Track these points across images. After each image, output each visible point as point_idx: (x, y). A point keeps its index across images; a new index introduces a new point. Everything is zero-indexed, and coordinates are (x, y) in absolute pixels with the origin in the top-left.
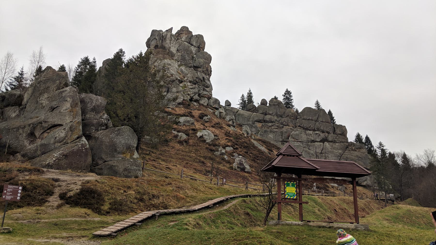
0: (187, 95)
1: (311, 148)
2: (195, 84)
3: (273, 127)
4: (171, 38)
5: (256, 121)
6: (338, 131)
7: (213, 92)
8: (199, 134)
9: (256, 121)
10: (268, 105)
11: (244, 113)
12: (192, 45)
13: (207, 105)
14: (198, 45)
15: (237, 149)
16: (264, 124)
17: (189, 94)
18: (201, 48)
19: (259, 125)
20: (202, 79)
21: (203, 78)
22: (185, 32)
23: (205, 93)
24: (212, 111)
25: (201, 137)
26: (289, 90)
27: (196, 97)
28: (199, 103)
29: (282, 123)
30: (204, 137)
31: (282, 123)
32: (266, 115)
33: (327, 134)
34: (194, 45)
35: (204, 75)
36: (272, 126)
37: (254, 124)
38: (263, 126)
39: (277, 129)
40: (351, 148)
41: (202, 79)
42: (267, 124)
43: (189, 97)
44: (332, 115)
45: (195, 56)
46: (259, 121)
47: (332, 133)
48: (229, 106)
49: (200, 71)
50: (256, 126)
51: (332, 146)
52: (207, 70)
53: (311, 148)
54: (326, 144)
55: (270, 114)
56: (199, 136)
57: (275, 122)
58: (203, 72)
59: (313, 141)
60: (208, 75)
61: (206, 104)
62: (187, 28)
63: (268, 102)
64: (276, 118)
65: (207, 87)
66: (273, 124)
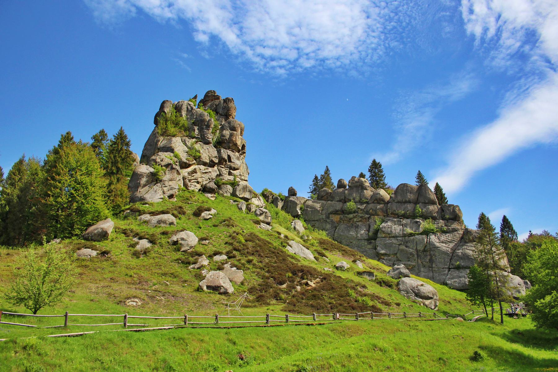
1: (409, 244)
3: (355, 220)
9: (331, 213)
10: (347, 187)
15: (234, 257)
16: (342, 216)
17: (198, 183)
19: (336, 218)
21: (229, 157)
26: (377, 161)
29: (367, 213)
32: (345, 202)
36: (354, 217)
37: (328, 218)
39: (361, 221)
42: (347, 215)
44: (441, 190)
46: (336, 212)
50: (332, 221)
53: (409, 244)
66: (355, 215)
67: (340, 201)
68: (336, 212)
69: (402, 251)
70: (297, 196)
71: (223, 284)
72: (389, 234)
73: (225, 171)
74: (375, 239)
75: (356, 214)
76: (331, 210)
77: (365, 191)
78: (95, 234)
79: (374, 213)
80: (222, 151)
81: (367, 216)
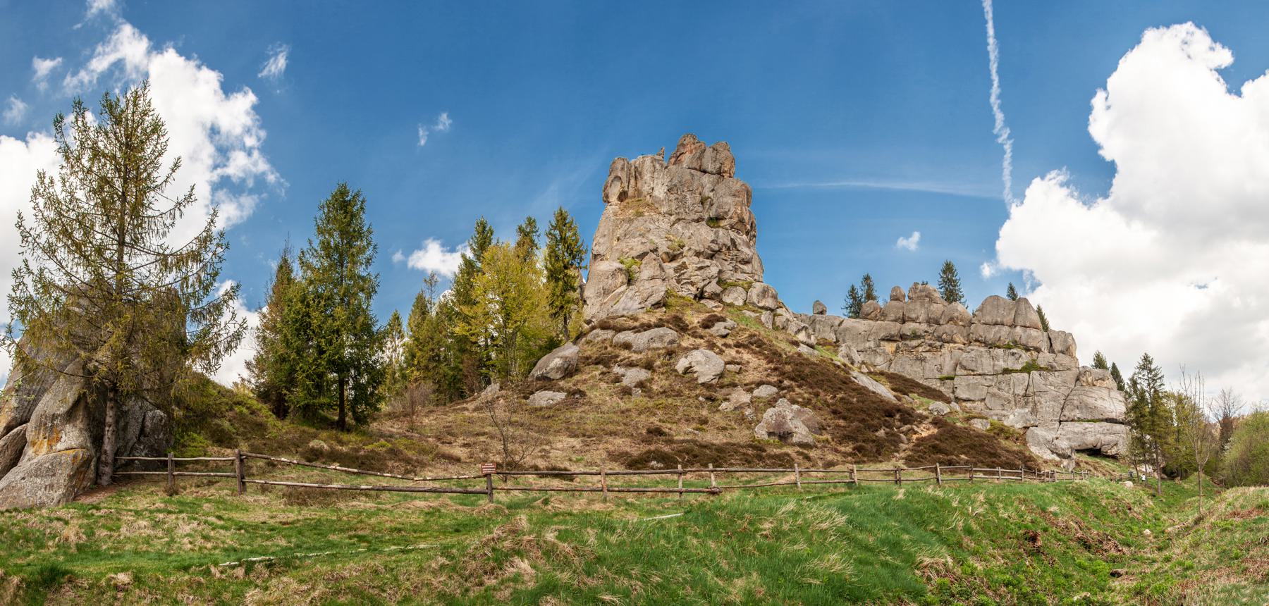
2: (711, 257)
3: (921, 349)
5: (883, 340)
13: (745, 303)
17: (692, 284)
19: (889, 347)
20: (729, 243)
24: (753, 315)
25: (688, 370)
27: (713, 287)
28: (721, 301)
29: (939, 338)
30: (695, 369)
31: (939, 338)
37: (879, 346)
38: (898, 348)
43: (693, 289)
46: (890, 339)
48: (822, 313)
55: (913, 321)
61: (740, 303)
64: (924, 326)
65: (746, 262)
67: (895, 321)
69: (994, 395)
73: (728, 267)
74: (952, 379)
76: (882, 335)
79: (949, 338)
81: (938, 344)
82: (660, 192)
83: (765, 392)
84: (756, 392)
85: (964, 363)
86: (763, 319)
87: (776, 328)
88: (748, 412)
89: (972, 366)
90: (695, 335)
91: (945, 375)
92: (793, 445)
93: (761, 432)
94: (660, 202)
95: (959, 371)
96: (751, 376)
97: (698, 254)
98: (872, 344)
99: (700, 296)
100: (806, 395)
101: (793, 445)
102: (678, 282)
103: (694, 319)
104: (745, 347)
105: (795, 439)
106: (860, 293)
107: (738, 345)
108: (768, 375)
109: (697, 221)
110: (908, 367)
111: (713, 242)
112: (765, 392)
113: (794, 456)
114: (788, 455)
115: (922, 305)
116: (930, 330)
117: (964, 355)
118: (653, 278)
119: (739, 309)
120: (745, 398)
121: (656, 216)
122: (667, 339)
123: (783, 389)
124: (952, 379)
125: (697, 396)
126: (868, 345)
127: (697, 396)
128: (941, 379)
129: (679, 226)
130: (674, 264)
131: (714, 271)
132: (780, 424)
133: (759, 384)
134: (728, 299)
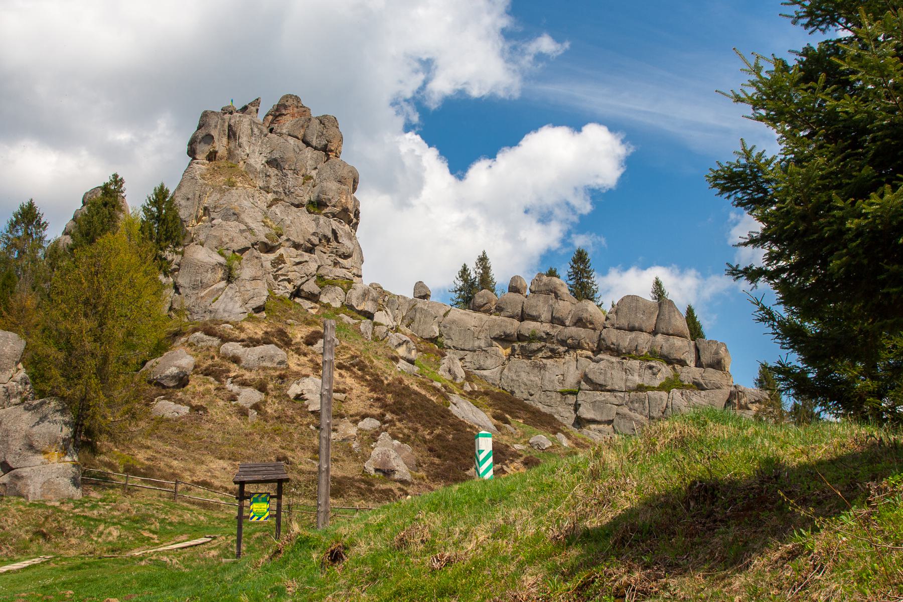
0: (286, 283)
2: (310, 250)
3: (540, 355)
4: (252, 129)
5: (495, 339)
6: (706, 358)
7: (365, 269)
8: (294, 390)
9: (495, 339)
11: (464, 317)
12: (308, 144)
14: (325, 142)
17: (289, 281)
18: (331, 151)
20: (330, 235)
21: (334, 232)
22: (290, 110)
23: (339, 272)
24: (352, 321)
25: (299, 397)
27: (311, 286)
29: (563, 342)
30: (307, 396)
31: (563, 342)
33: (678, 367)
34: (314, 144)
35: (334, 224)
38: (513, 350)
40: (736, 401)
41: (330, 235)
43: (290, 288)
45: (314, 173)
46: (504, 339)
47: (692, 364)
49: (326, 215)
51: (689, 399)
52: (345, 210)
54: (676, 393)
56: (292, 396)
57: (545, 340)
58: (334, 216)
59: (641, 388)
60: (349, 222)
61: (337, 304)
62: (297, 99)
63: (529, 285)
64: (547, 327)
65: (346, 257)
68: (504, 339)
70: (431, 299)
71: (397, 468)
72: (601, 385)
73: (327, 260)
75: (543, 343)
76: (497, 332)
77: (561, 302)
78: (167, 376)
80: (321, 221)
81: (562, 349)
82: (258, 161)
83: (369, 424)
84: (360, 424)
85: (591, 376)
86: (362, 327)
87: (376, 339)
88: (355, 445)
89: (600, 379)
90: (298, 352)
91: (568, 387)
92: (396, 481)
93: (370, 467)
94: (255, 171)
95: (584, 385)
96: (356, 406)
97: (296, 246)
98: (482, 344)
99: (297, 293)
100: (406, 431)
101: (396, 481)
102: (276, 278)
103: (299, 333)
104: (347, 369)
105: (397, 476)
106: (473, 275)
107: (340, 367)
108: (371, 406)
109: (298, 206)
110: (523, 375)
111: (314, 234)
112: (369, 424)
113: (396, 491)
114: (391, 490)
115: (546, 301)
116: (553, 332)
117: (592, 365)
118: (254, 279)
119: (337, 311)
120: (353, 431)
121: (251, 190)
122: (277, 360)
123: (385, 423)
124: (575, 393)
125: (308, 424)
126: (477, 343)
127: (308, 424)
128: (562, 393)
129: (277, 209)
130: (272, 256)
131: (312, 267)
132: (385, 463)
133: (364, 417)
134: (324, 299)
